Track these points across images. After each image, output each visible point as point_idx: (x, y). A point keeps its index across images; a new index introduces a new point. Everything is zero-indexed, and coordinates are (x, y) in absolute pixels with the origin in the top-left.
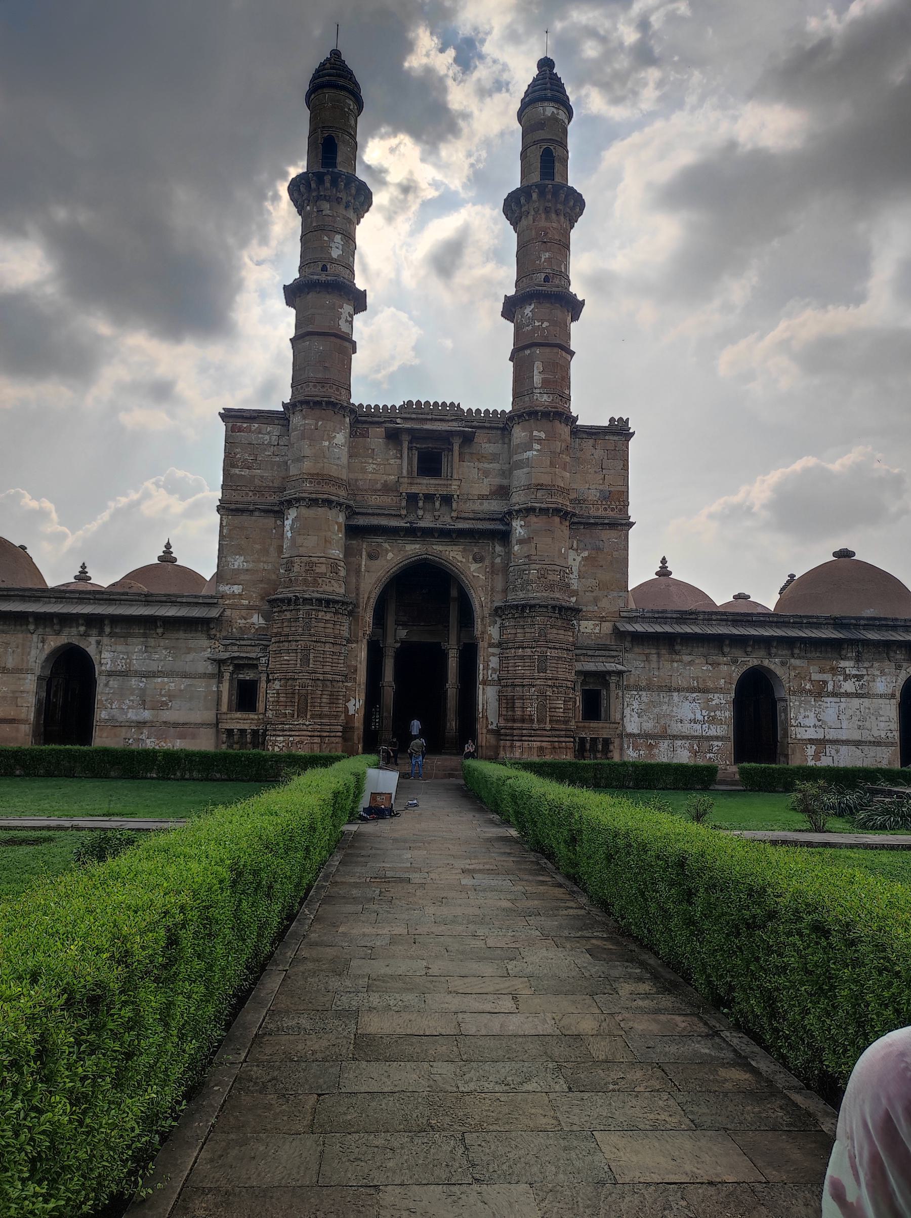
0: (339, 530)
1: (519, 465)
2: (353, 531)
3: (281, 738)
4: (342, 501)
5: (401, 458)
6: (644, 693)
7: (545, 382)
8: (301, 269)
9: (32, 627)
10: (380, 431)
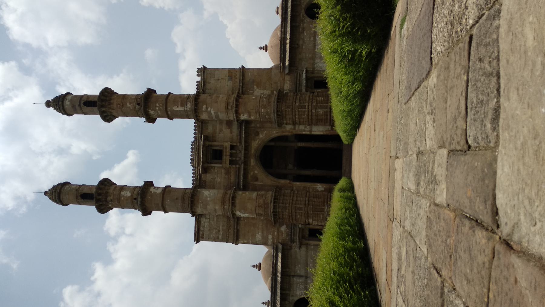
0: (245, 193)
1: (217, 116)
2: (245, 188)
4: (232, 192)
5: (215, 167)
6: (316, 61)
7: (182, 105)
8: (136, 209)
10: (203, 176)
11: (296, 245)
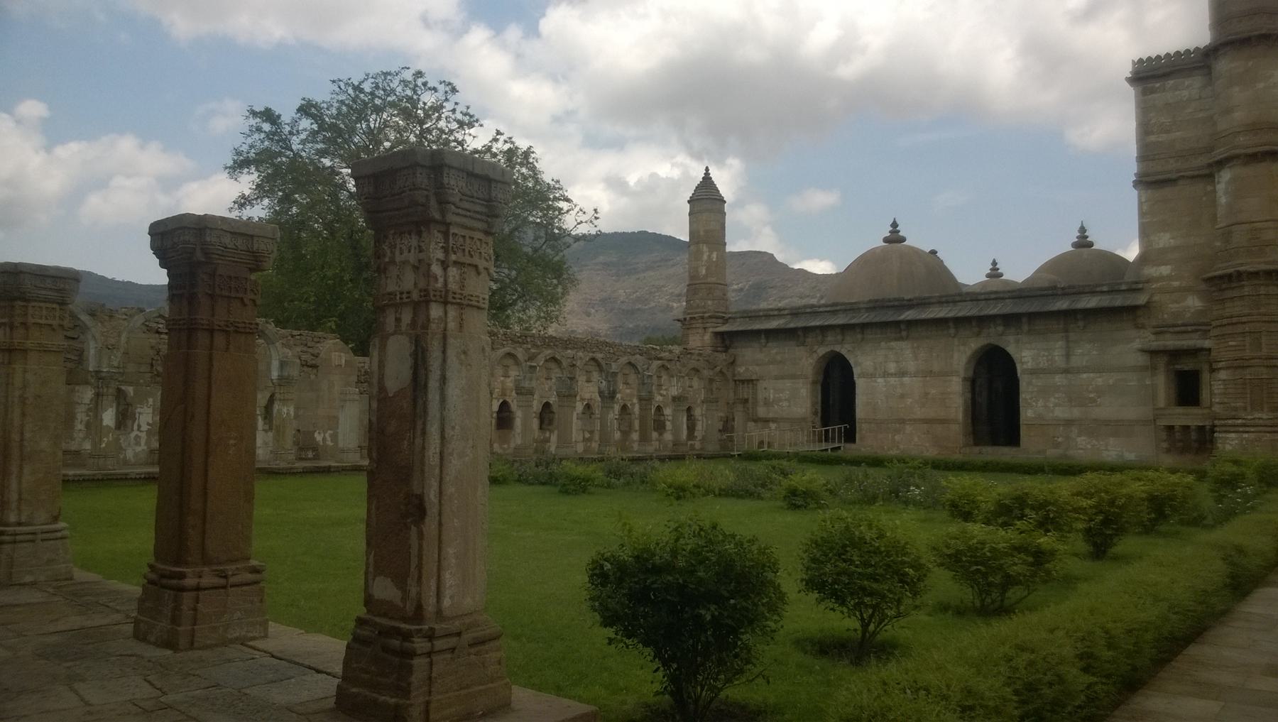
3: (1233, 435)
9: (952, 331)
11: (1146, 338)
